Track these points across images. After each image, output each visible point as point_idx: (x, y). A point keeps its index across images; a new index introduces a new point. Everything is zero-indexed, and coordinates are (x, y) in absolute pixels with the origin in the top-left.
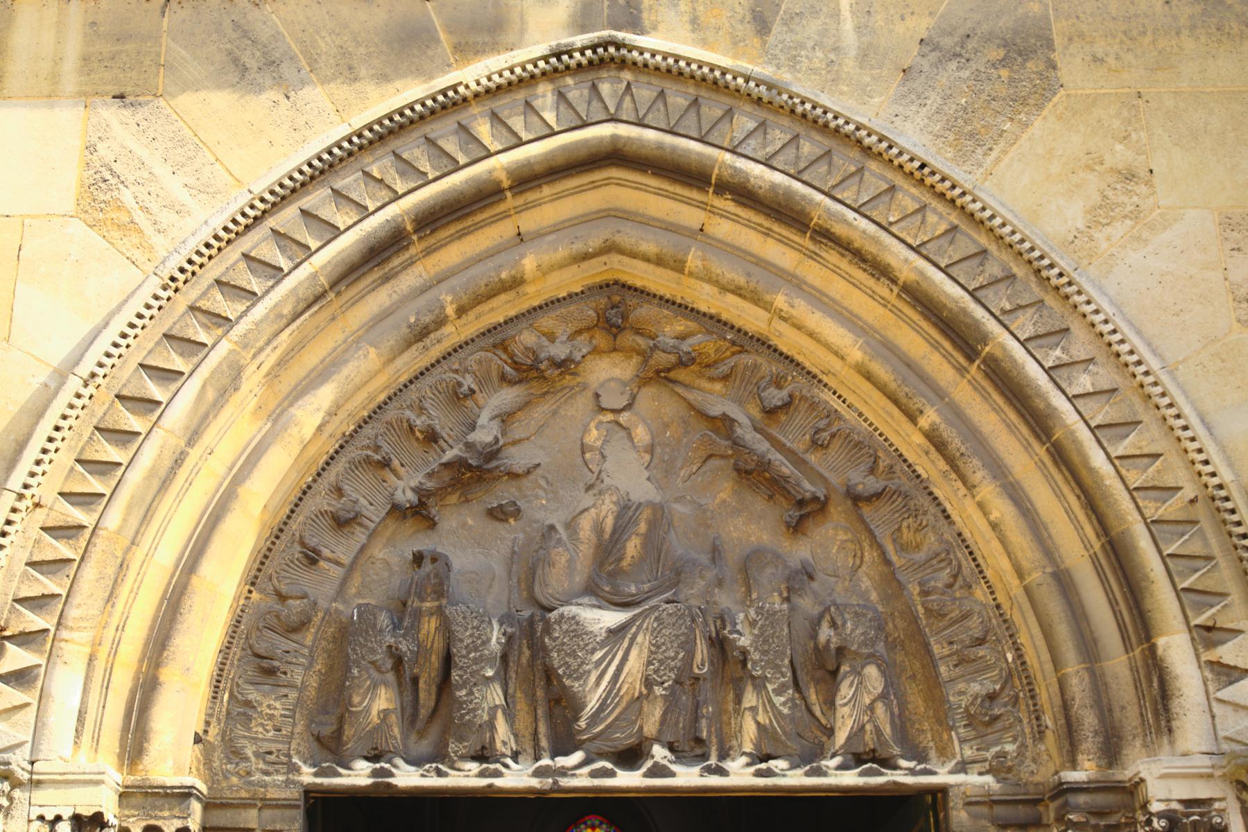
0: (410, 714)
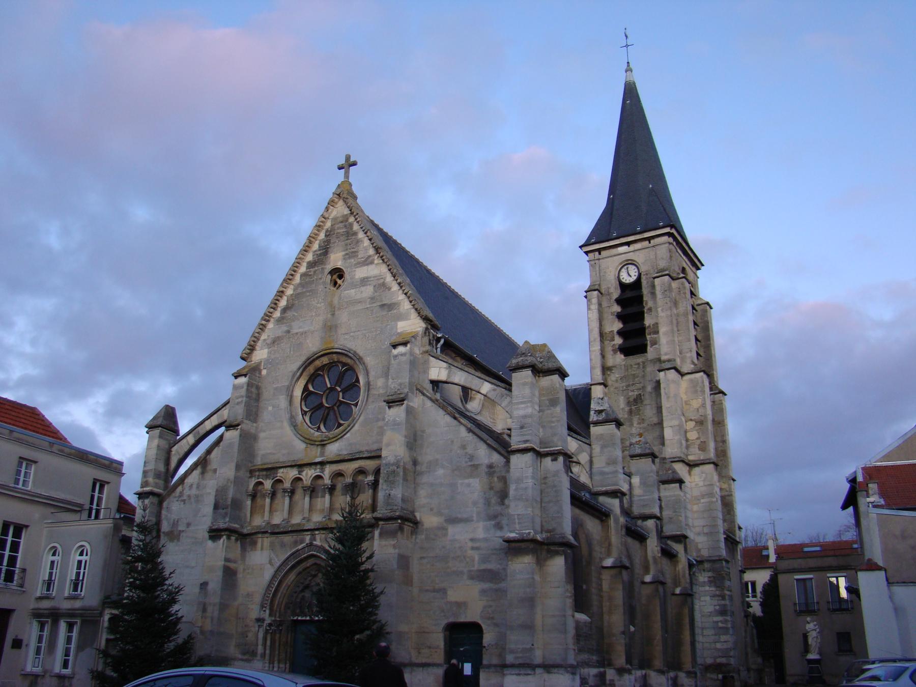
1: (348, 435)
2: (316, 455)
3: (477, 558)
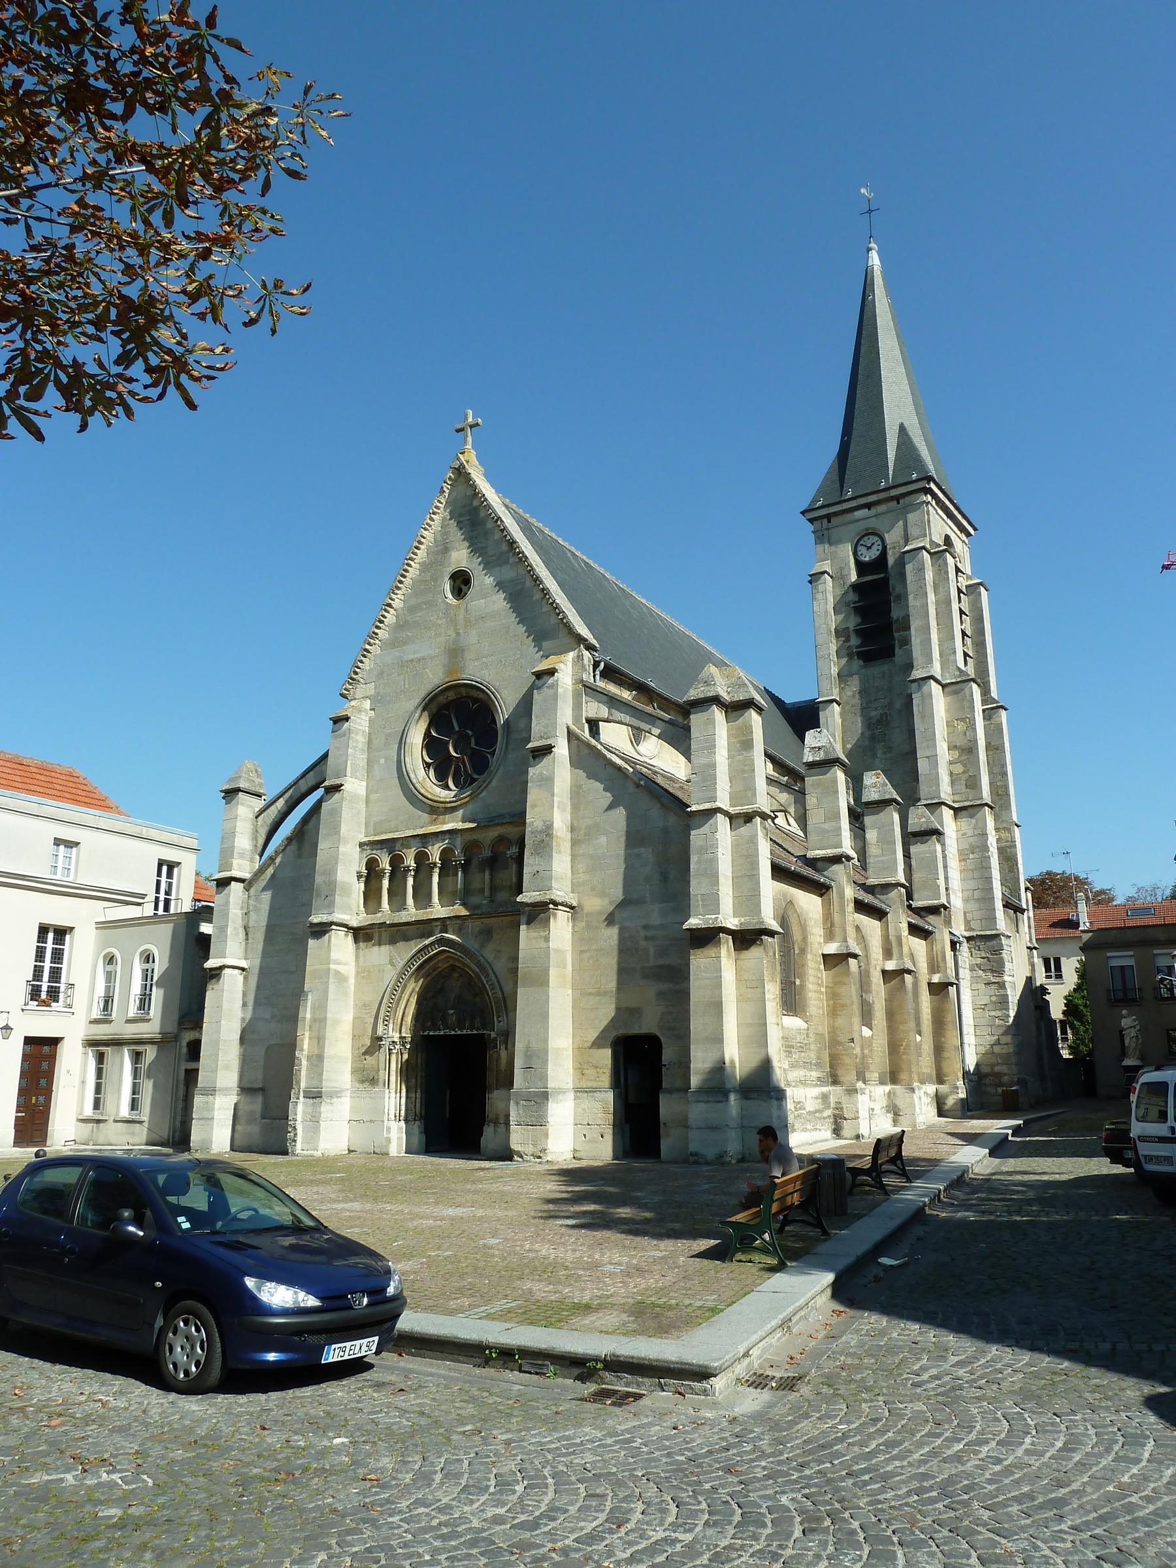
1: (484, 794)
3: (652, 950)
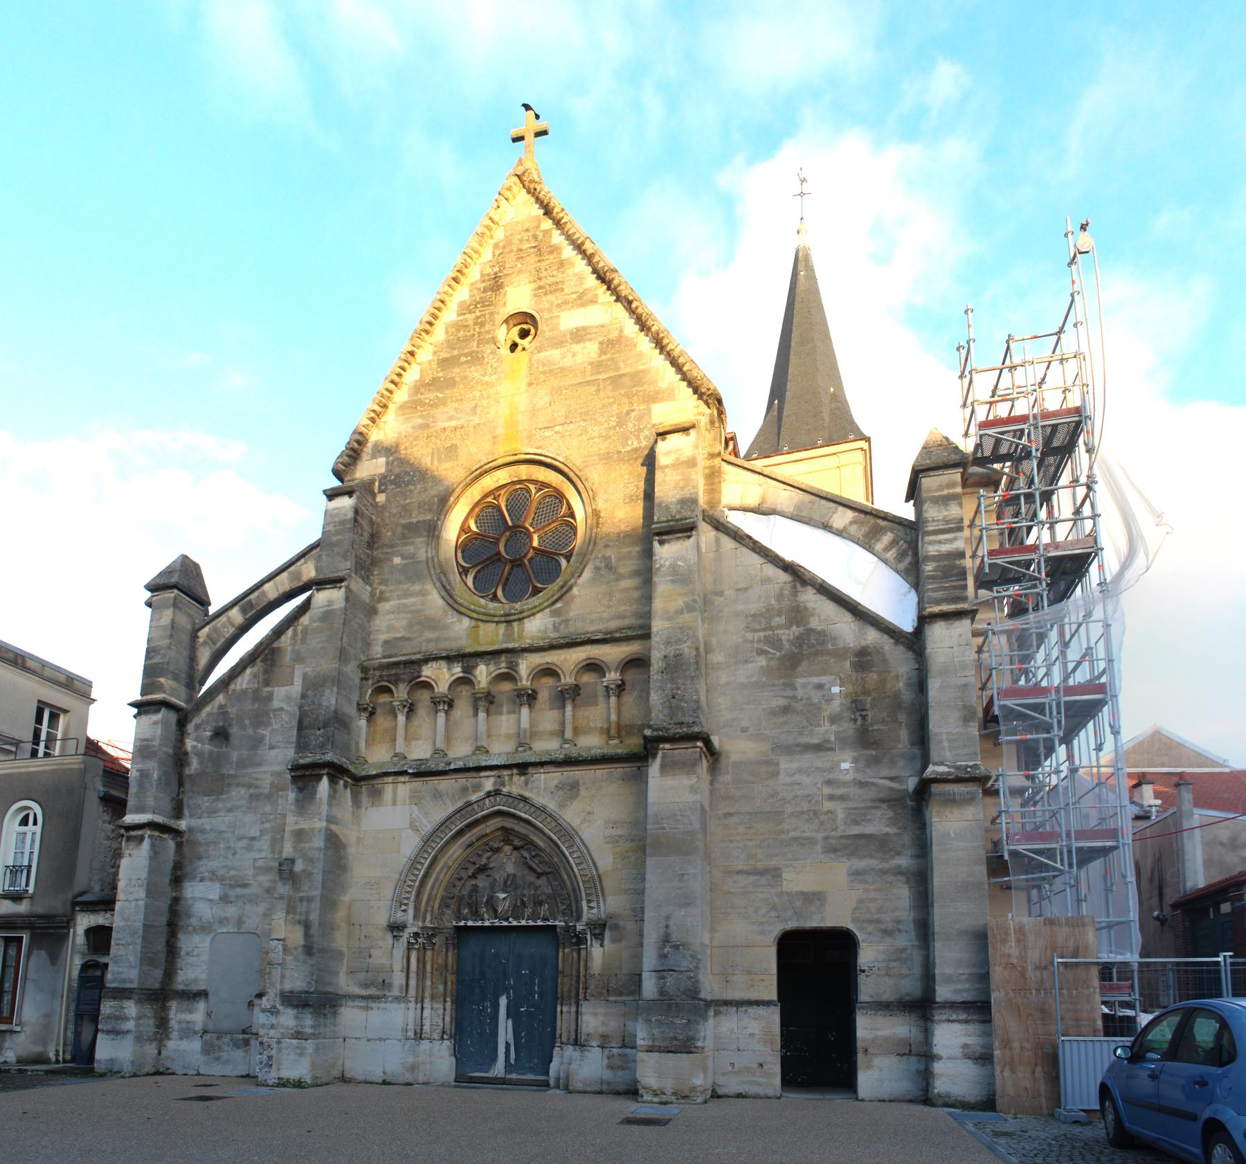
0: (471, 913)
2: (492, 636)
